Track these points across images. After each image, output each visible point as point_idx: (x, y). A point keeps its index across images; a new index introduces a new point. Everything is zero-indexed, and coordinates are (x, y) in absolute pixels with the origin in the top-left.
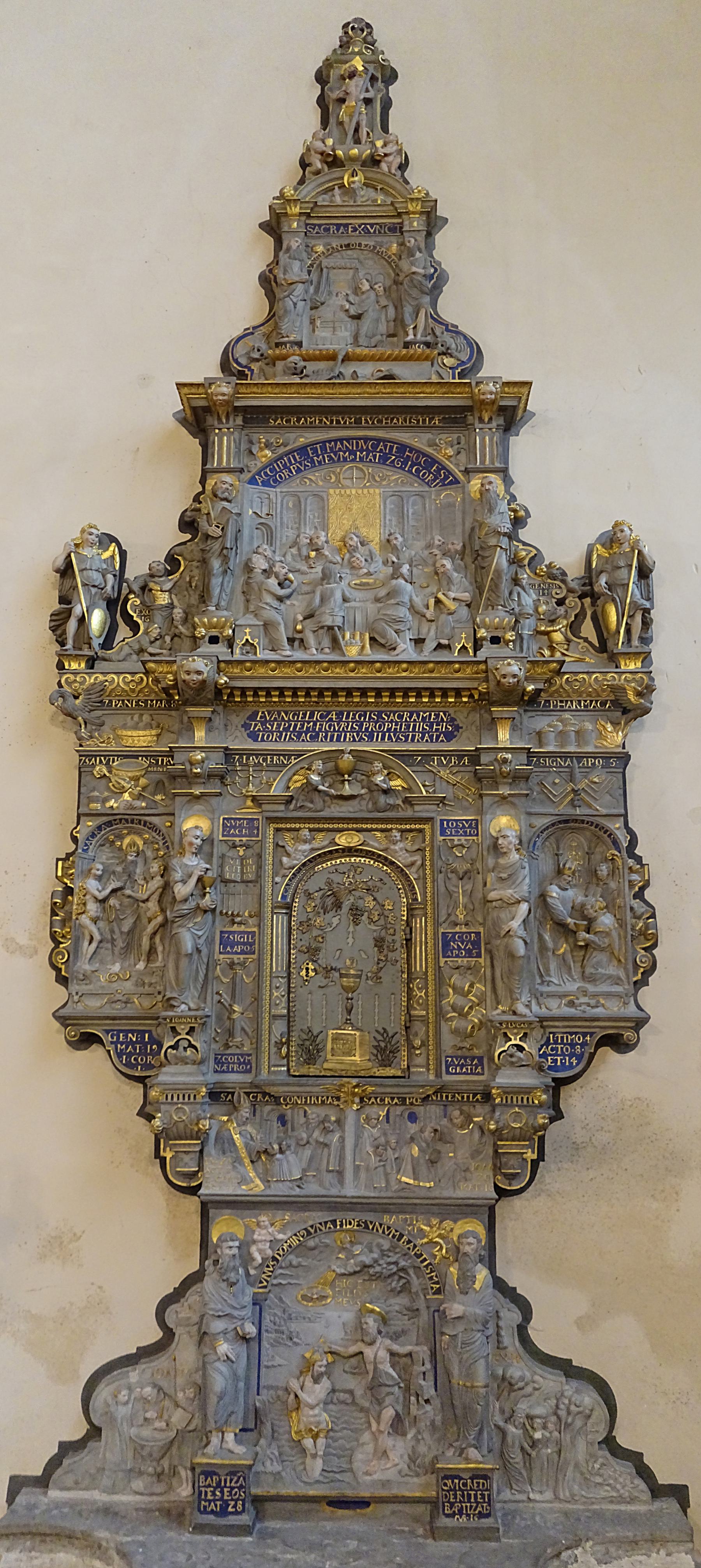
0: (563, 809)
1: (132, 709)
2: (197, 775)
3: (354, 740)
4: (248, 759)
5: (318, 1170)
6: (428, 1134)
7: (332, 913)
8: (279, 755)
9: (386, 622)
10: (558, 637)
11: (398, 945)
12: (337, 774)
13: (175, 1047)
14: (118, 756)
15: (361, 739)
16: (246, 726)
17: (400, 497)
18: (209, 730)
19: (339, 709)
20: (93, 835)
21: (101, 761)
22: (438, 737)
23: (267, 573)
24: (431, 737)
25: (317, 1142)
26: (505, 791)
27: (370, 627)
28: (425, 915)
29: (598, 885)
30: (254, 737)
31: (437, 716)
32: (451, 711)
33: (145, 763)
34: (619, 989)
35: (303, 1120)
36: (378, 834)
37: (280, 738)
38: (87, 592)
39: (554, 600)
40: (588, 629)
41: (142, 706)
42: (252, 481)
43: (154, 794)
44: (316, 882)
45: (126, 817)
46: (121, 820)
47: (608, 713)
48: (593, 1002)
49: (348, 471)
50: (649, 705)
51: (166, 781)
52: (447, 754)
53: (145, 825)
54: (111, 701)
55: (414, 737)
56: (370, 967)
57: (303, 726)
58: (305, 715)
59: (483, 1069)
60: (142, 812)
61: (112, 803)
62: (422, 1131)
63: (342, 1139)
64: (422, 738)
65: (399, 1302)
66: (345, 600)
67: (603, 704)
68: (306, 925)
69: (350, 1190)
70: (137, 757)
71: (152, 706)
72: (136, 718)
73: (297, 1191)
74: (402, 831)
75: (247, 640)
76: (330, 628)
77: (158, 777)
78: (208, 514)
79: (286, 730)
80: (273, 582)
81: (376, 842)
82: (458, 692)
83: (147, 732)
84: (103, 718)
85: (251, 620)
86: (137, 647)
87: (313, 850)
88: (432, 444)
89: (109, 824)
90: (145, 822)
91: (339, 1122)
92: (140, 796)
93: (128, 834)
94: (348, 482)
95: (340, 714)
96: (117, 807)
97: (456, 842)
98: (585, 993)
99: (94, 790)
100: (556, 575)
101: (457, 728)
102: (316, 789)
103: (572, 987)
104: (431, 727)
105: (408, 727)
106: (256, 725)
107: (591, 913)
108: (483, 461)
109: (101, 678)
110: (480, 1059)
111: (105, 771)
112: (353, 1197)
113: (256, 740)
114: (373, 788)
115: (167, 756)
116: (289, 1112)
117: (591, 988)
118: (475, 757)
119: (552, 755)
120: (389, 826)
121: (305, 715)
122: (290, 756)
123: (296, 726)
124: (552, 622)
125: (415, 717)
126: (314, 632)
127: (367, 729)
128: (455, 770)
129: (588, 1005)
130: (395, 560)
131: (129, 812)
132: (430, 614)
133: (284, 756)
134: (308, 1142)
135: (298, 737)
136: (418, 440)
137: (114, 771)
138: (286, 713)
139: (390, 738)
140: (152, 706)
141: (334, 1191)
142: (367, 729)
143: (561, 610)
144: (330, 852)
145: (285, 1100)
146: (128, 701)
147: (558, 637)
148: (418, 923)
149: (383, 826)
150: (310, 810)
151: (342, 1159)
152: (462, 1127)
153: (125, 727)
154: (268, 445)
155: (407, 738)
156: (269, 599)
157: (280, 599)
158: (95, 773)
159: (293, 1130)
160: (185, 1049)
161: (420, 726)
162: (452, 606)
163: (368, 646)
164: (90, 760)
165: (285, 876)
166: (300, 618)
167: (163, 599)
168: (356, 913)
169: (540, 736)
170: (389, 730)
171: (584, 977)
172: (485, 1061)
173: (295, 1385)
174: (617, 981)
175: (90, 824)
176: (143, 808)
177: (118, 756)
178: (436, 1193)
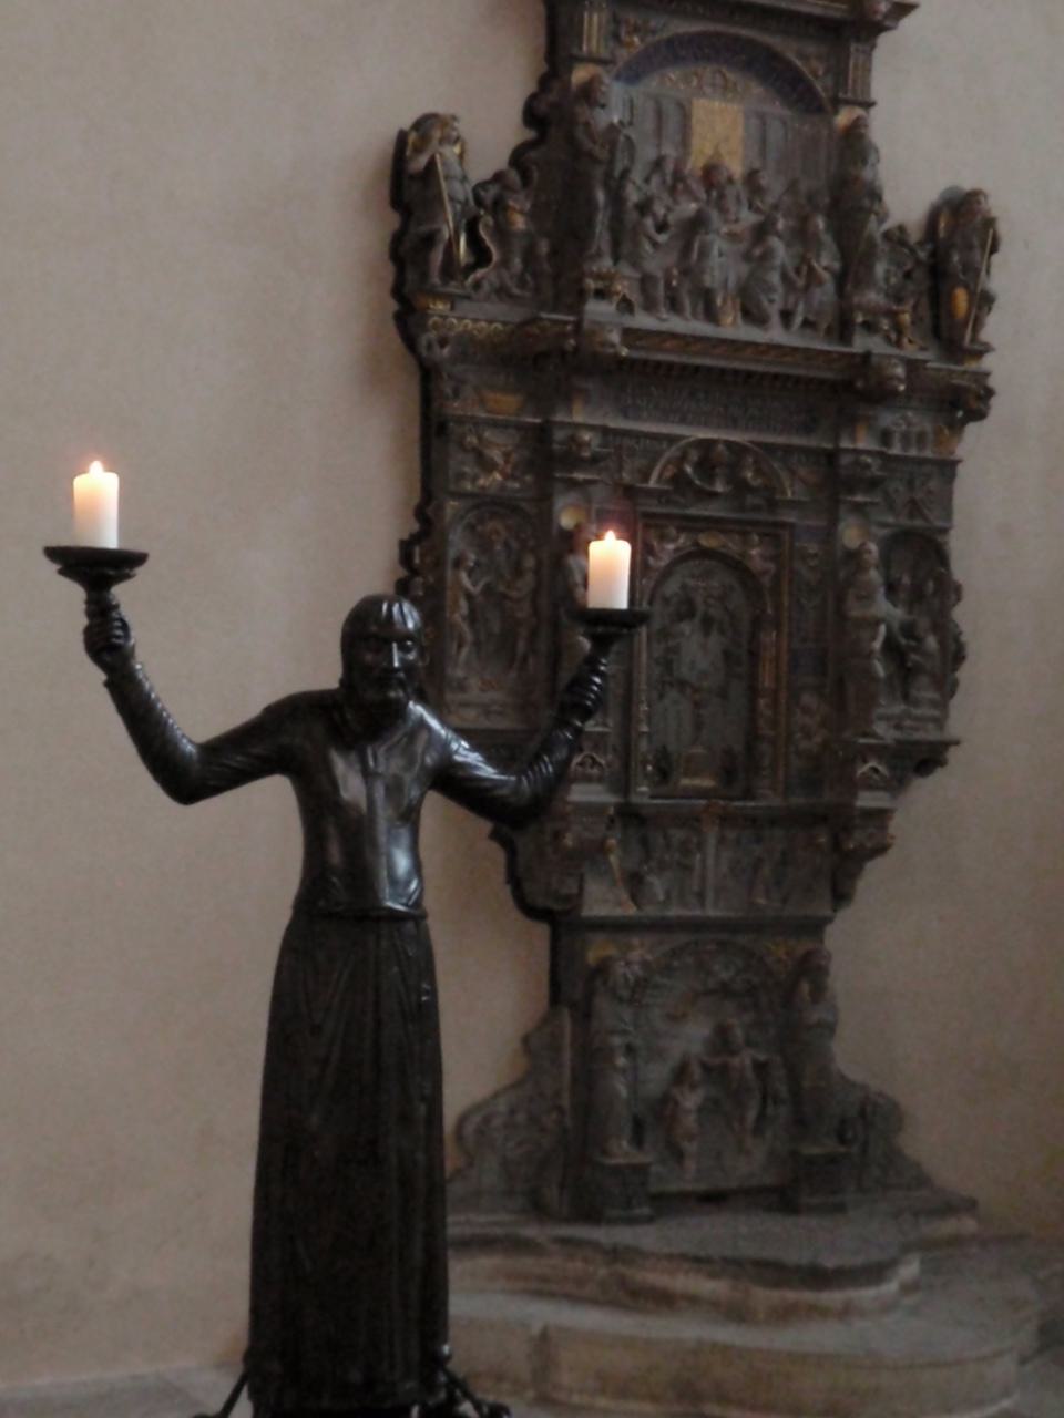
0: (905, 521)
2: (583, 460)
10: (906, 318)
12: (707, 466)
13: (581, 764)
17: (762, 117)
20: (462, 518)
21: (470, 430)
23: (644, 207)
26: (859, 498)
30: (625, 414)
34: (936, 713)
38: (454, 207)
40: (925, 311)
42: (618, 77)
44: (672, 587)
49: (708, 71)
50: (982, 406)
61: (482, 482)
63: (703, 861)
65: (748, 1017)
66: (721, 254)
68: (664, 634)
69: (711, 912)
78: (587, 124)
80: (649, 222)
81: (732, 546)
85: (625, 269)
87: (677, 550)
88: (804, 57)
91: (701, 846)
92: (513, 477)
94: (708, 90)
97: (811, 551)
98: (909, 716)
100: (897, 238)
102: (690, 483)
103: (898, 708)
108: (854, 91)
117: (918, 712)
118: (831, 457)
119: (897, 458)
124: (899, 300)
130: (759, 203)
136: (789, 48)
141: (698, 912)
143: (911, 287)
147: (906, 318)
148: (768, 637)
151: (703, 878)
154: (636, 30)
156: (647, 247)
157: (655, 244)
160: (592, 767)
162: (826, 276)
163: (739, 314)
166: (675, 272)
167: (520, 223)
169: (886, 437)
171: (906, 697)
173: (675, 1092)
174: (933, 704)
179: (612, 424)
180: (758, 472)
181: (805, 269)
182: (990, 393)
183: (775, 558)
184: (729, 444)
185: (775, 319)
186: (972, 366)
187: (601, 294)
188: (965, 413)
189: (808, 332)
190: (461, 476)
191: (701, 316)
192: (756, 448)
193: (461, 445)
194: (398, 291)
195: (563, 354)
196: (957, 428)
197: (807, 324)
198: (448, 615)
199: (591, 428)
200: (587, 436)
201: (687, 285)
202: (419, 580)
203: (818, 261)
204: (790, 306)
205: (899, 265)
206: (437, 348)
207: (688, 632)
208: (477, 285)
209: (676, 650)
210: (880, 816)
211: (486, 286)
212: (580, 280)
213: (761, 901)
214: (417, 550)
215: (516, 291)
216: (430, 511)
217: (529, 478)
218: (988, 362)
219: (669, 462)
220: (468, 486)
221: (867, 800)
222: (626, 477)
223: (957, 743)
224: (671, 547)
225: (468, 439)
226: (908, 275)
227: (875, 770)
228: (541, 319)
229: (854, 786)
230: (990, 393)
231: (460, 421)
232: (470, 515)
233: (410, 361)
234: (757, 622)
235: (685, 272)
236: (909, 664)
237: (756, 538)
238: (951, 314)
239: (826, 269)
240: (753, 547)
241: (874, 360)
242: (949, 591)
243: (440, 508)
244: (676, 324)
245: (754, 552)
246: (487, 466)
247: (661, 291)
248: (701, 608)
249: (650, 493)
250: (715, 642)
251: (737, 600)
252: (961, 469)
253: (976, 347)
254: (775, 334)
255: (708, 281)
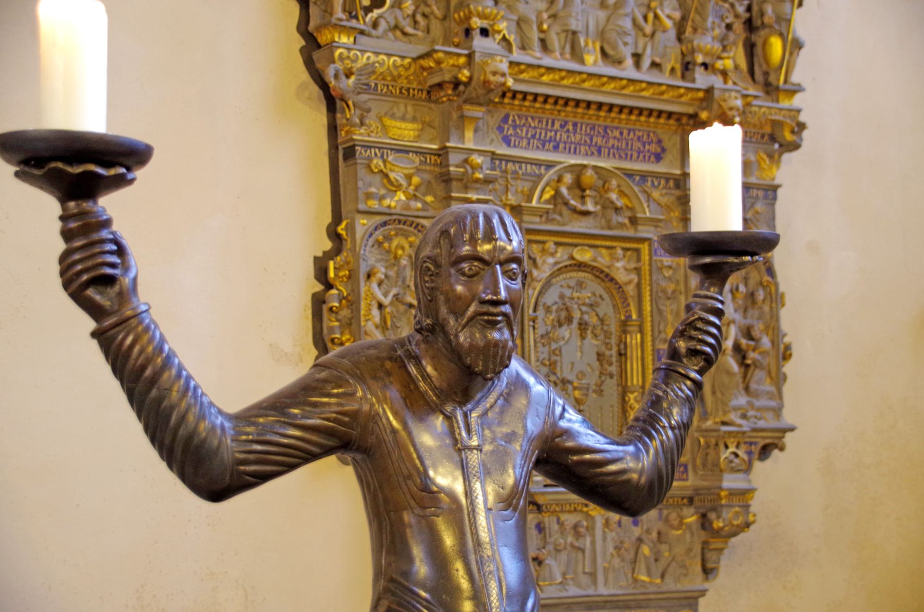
1: (396, 97)
2: (477, 181)
3: (587, 154)
4: (506, 165)
5: (575, 572)
6: (654, 535)
7: (565, 327)
8: (532, 164)
9: (618, 33)
11: (614, 359)
12: (579, 187)
14: (392, 149)
15: (592, 154)
16: (500, 129)
18: (476, 131)
19: (574, 120)
21: (376, 154)
22: (649, 157)
24: (644, 157)
25: (572, 545)
27: (602, 35)
28: (641, 331)
29: (753, 308)
30: (507, 141)
31: (649, 136)
32: (659, 131)
33: (417, 159)
34: (773, 404)
35: (556, 527)
36: (604, 251)
37: (529, 144)
39: (724, 25)
41: (406, 93)
43: (425, 194)
44: (551, 297)
45: (401, 218)
46: (395, 220)
47: (765, 146)
48: (758, 414)
51: (433, 181)
52: (657, 175)
53: (415, 228)
54: (376, 85)
55: (632, 155)
56: (592, 380)
57: (546, 134)
58: (547, 122)
59: (687, 475)
60: (416, 213)
62: (648, 531)
63: (593, 543)
64: (638, 157)
67: (763, 136)
69: (602, 590)
70: (407, 152)
71: (414, 95)
72: (402, 108)
73: (564, 594)
74: (625, 250)
75: (504, 36)
76: (574, 33)
77: (427, 176)
79: (534, 136)
81: (603, 259)
82: (670, 115)
83: (410, 126)
84: (370, 104)
86: (393, 23)
87: (556, 263)
89: (385, 224)
90: (418, 225)
91: (591, 529)
92: (415, 197)
93: (396, 235)
95: (575, 125)
96: (395, 207)
99: (370, 185)
101: (663, 150)
102: (566, 204)
104: (644, 146)
105: (627, 144)
106: (508, 129)
107: (756, 333)
109: (373, 58)
110: (686, 466)
111: (381, 163)
112: (609, 596)
113: (509, 145)
114: (608, 206)
115: (435, 155)
116: (546, 520)
117: (758, 403)
120: (614, 244)
121: (547, 122)
122: (540, 165)
123: (541, 133)
125: (632, 134)
126: (558, 34)
127: (596, 143)
128: (664, 191)
129: (756, 417)
131: (405, 212)
132: (648, 29)
133: (536, 164)
134: (565, 548)
135: (544, 146)
137: (388, 166)
138: (532, 118)
139: (614, 155)
140: (414, 95)
141: (591, 591)
142: (596, 143)
144: (566, 267)
145: (546, 508)
146: (393, 86)
148: (634, 340)
149: (608, 243)
150: (559, 224)
152: (678, 529)
153: (393, 116)
155: (626, 155)
158: (373, 167)
159: (550, 536)
161: (636, 145)
162: (669, 23)
164: (366, 151)
165: (535, 289)
166: (545, 16)
168: (583, 326)
170: (613, 146)
172: (690, 467)
174: (771, 396)
175: (365, 221)
176: (418, 210)
177: (392, 149)
178: (664, 589)
179: (498, 152)
180: (622, 193)
181: (651, 16)
182: (802, 126)
183: (638, 270)
184: (595, 168)
185: (629, 62)
186: (785, 103)
187: (484, 32)
188: (781, 146)
189: (655, 71)
190: (369, 196)
191: (568, 56)
192: (617, 172)
193: (369, 167)
194: (303, 28)
195: (456, 84)
196: (774, 159)
197: (655, 65)
198: (363, 324)
199: (481, 152)
200: (478, 159)
201: (556, 28)
202: (334, 292)
203: (662, 10)
204: (640, 51)
205: (722, 18)
206: (344, 78)
207: (567, 335)
208: (375, 25)
209: (557, 352)
210: (743, 495)
211: (383, 25)
212: (468, 18)
213: (644, 578)
214: (331, 264)
215: (409, 30)
216: (341, 229)
217: (429, 199)
218: (797, 101)
219: (547, 184)
220: (373, 204)
221: (730, 482)
222: (512, 199)
223: (792, 429)
224: (551, 260)
225: (375, 161)
226: (729, 27)
227: (736, 455)
228: (436, 51)
229: (716, 469)
230: (802, 126)
231: (367, 147)
232: (377, 232)
233: (315, 89)
234: (624, 325)
235: (554, 16)
236: (749, 362)
237: (620, 252)
238: (767, 60)
239: (669, 17)
240: (618, 260)
241: (717, 94)
242: (776, 299)
243: (351, 228)
244: (547, 61)
245: (619, 264)
246: (394, 187)
247: (535, 35)
248: (577, 315)
249: (534, 211)
250: (592, 343)
251: (606, 308)
252: (780, 192)
253: (787, 87)
254: (628, 70)
255: (574, 25)
